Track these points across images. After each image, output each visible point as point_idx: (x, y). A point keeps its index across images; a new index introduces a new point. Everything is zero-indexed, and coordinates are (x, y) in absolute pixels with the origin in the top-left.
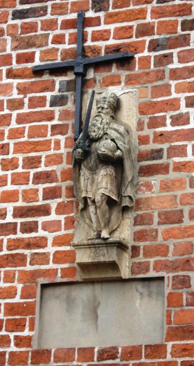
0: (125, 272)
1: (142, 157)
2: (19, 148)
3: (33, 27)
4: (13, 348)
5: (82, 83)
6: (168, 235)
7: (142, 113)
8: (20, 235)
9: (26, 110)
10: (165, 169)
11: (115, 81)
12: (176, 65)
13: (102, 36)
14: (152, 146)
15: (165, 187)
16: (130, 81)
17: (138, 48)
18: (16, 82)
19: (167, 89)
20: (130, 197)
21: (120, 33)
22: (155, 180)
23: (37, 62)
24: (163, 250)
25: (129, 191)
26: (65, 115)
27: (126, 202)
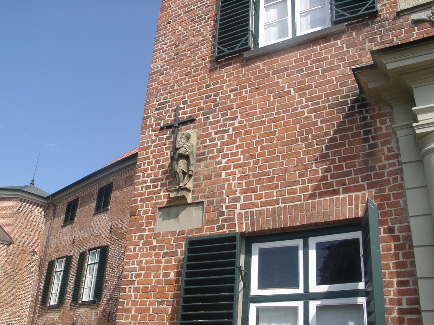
0: (189, 201)
3: (162, 113)
4: (147, 233)
6: (207, 185)
7: (198, 139)
8: (152, 189)
9: (157, 143)
10: (206, 159)
12: (211, 120)
14: (202, 151)
15: (206, 166)
16: (194, 128)
17: (197, 116)
20: (192, 171)
22: (202, 164)
24: (203, 191)
25: (192, 168)
27: (190, 173)
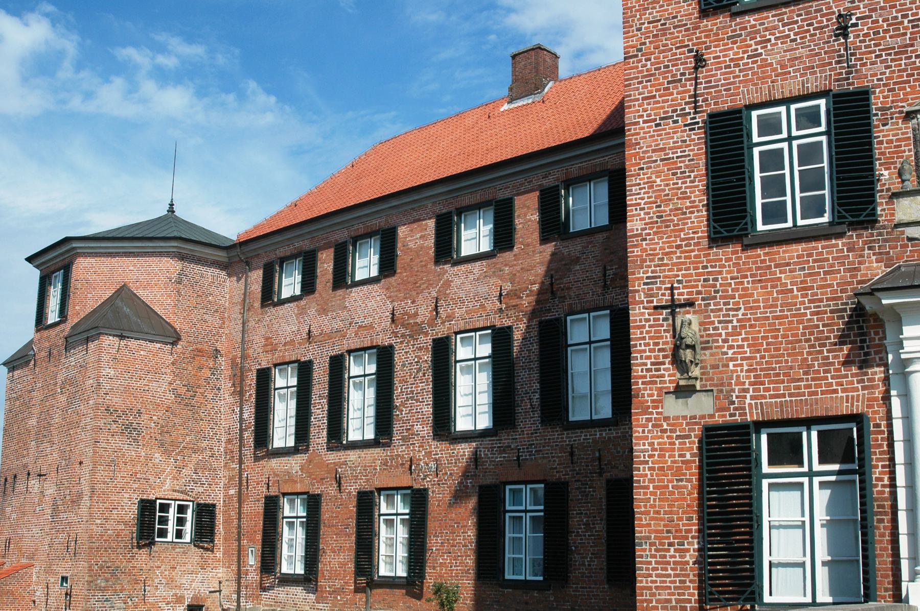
1: (702, 343)
2: (650, 338)
3: (652, 289)
5: (673, 314)
6: (714, 373)
9: (652, 323)
10: (711, 348)
11: (688, 313)
12: (712, 307)
13: (681, 294)
14: (705, 339)
15: (712, 355)
16: (694, 313)
17: (697, 300)
18: (647, 311)
19: (709, 317)
21: (689, 293)
22: (707, 352)
23: (655, 304)
24: (712, 379)
25: (698, 357)
26: (668, 325)
